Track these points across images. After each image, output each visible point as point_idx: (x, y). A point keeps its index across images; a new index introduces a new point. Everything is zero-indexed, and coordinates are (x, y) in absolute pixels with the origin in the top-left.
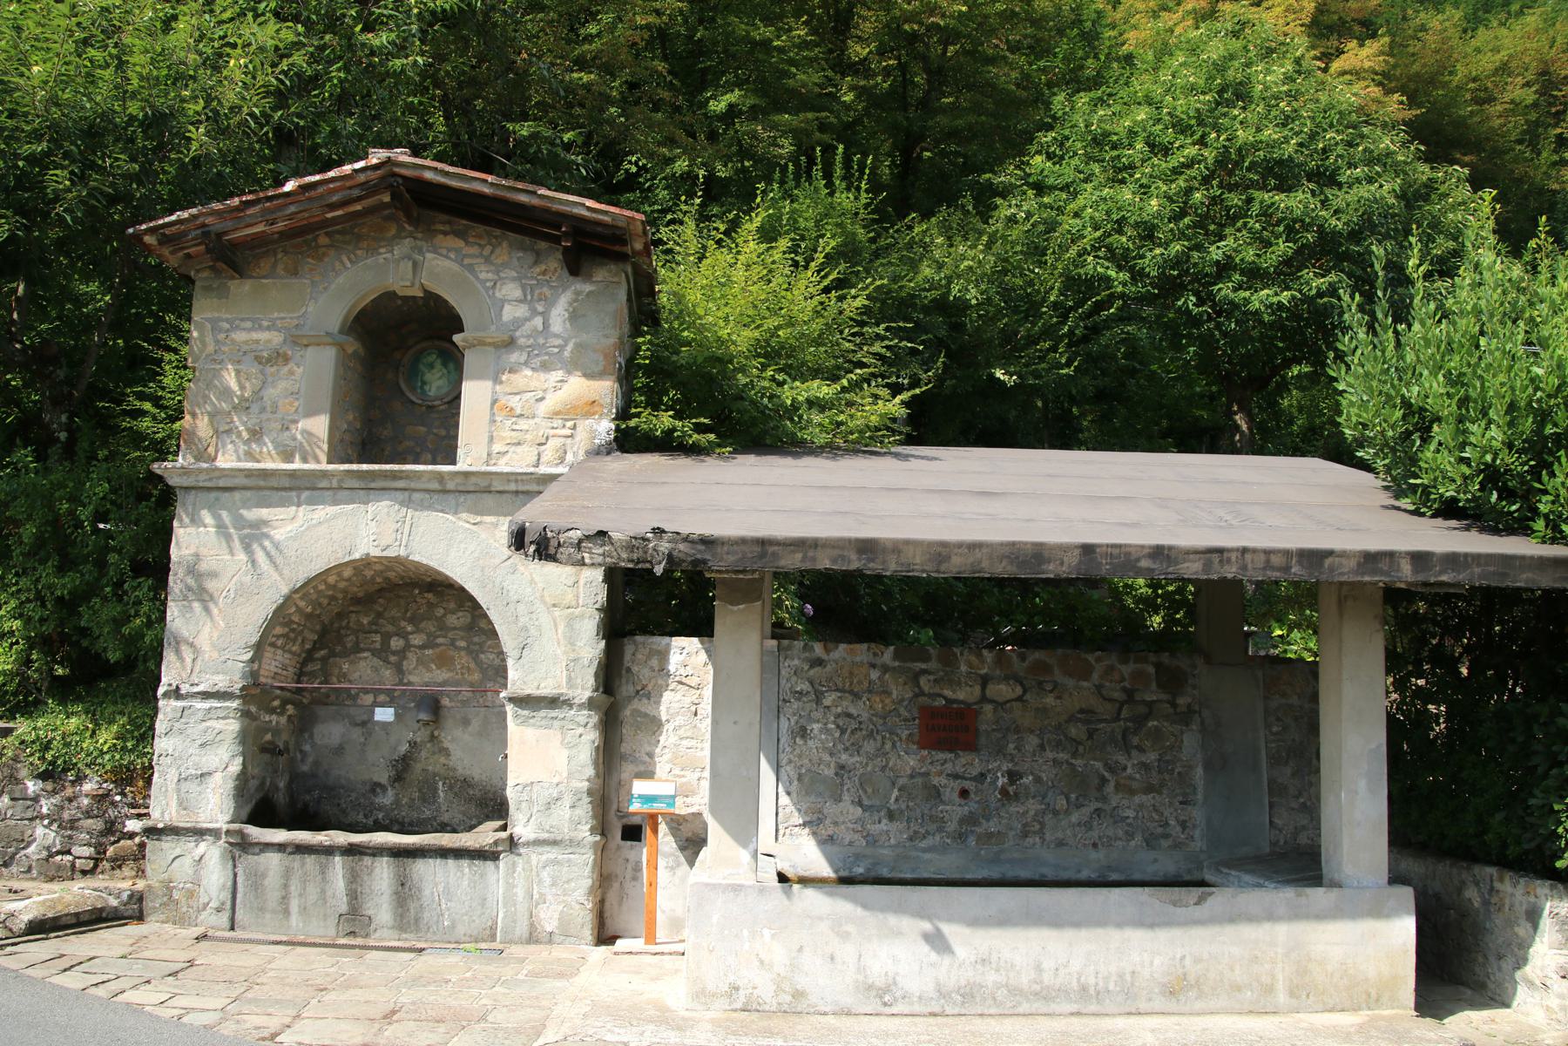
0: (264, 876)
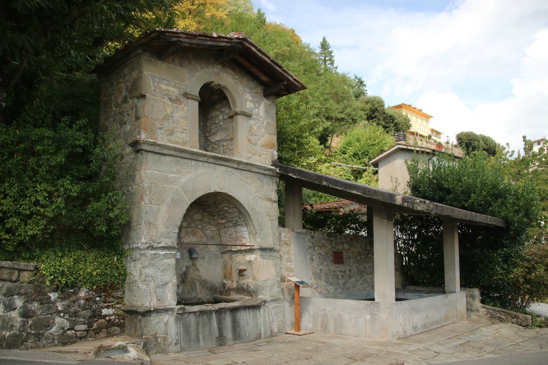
0: (190, 326)
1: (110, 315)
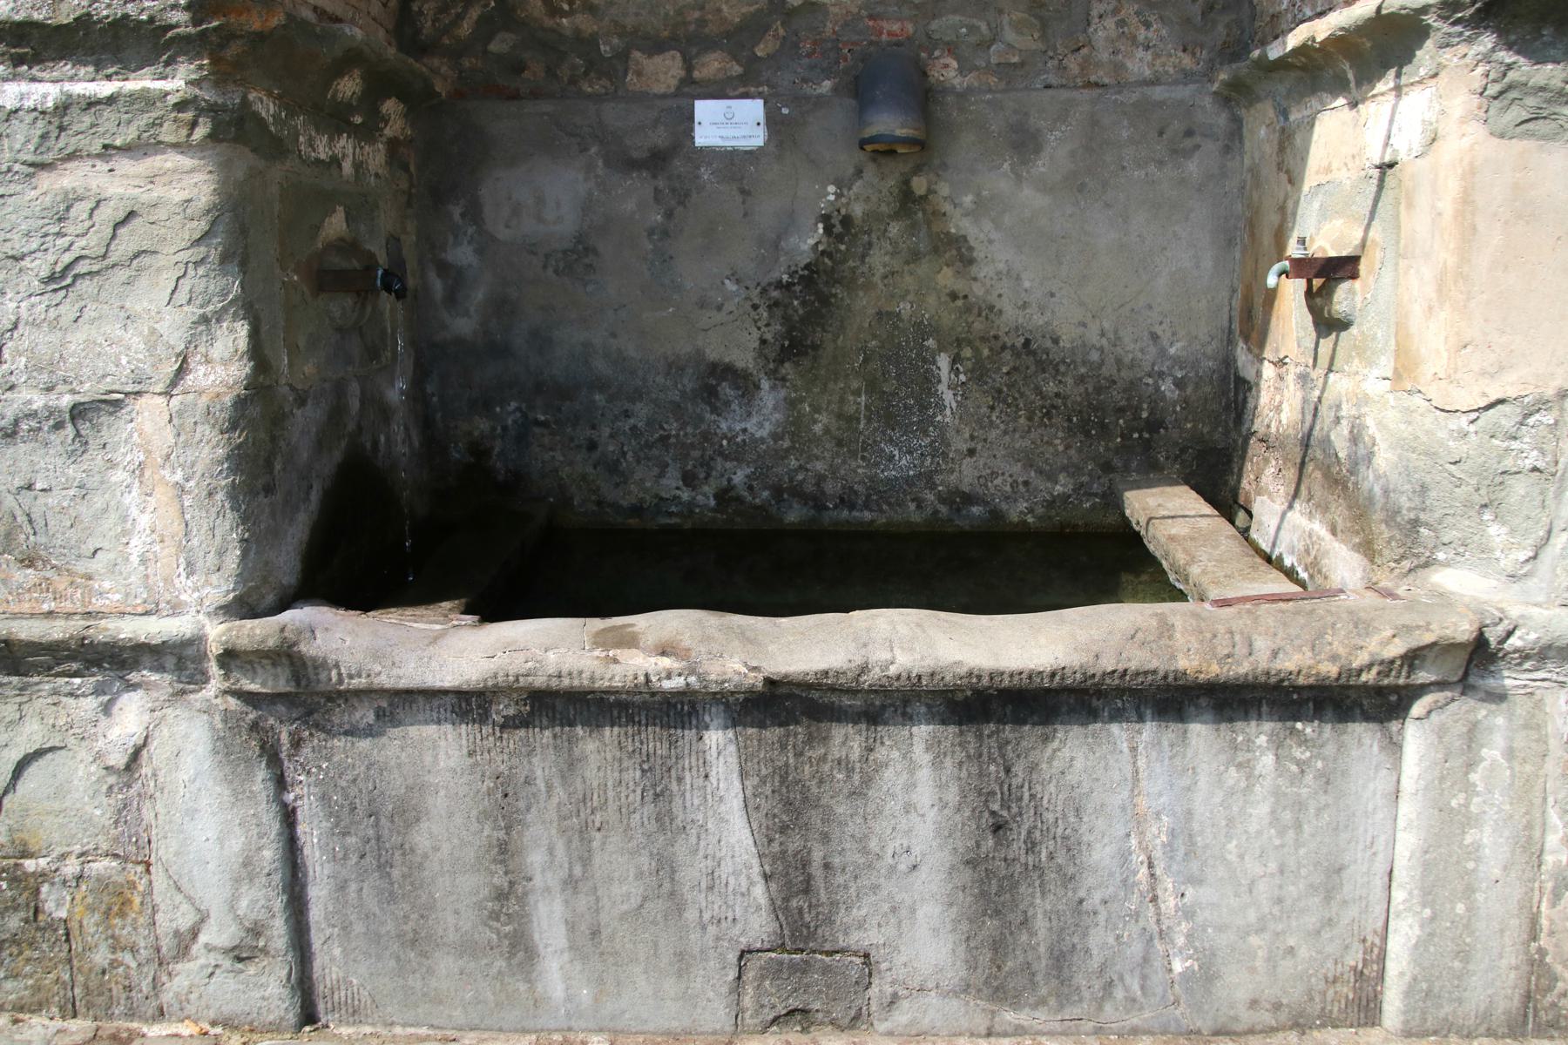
0: (408, 813)
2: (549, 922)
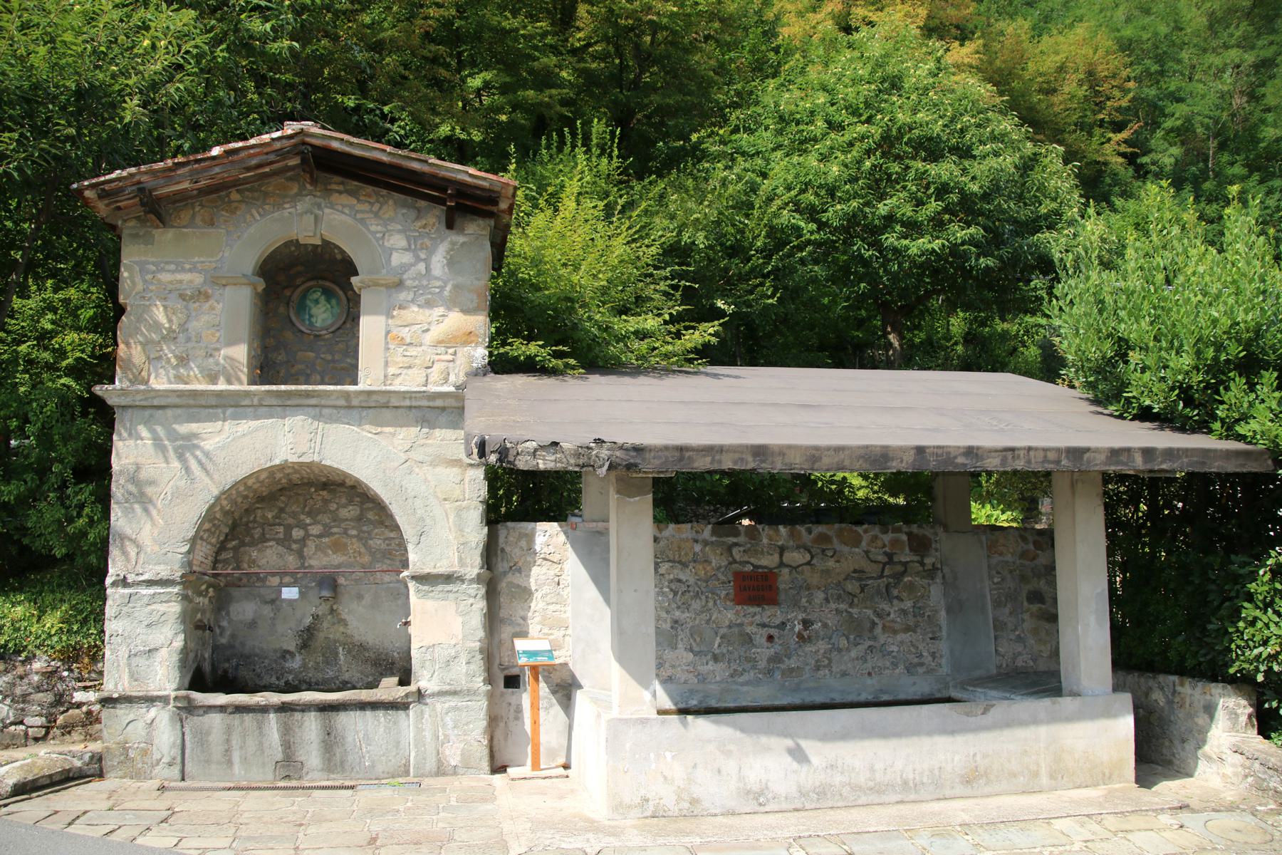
0: (208, 733)
1: (89, 703)
2: (236, 757)
